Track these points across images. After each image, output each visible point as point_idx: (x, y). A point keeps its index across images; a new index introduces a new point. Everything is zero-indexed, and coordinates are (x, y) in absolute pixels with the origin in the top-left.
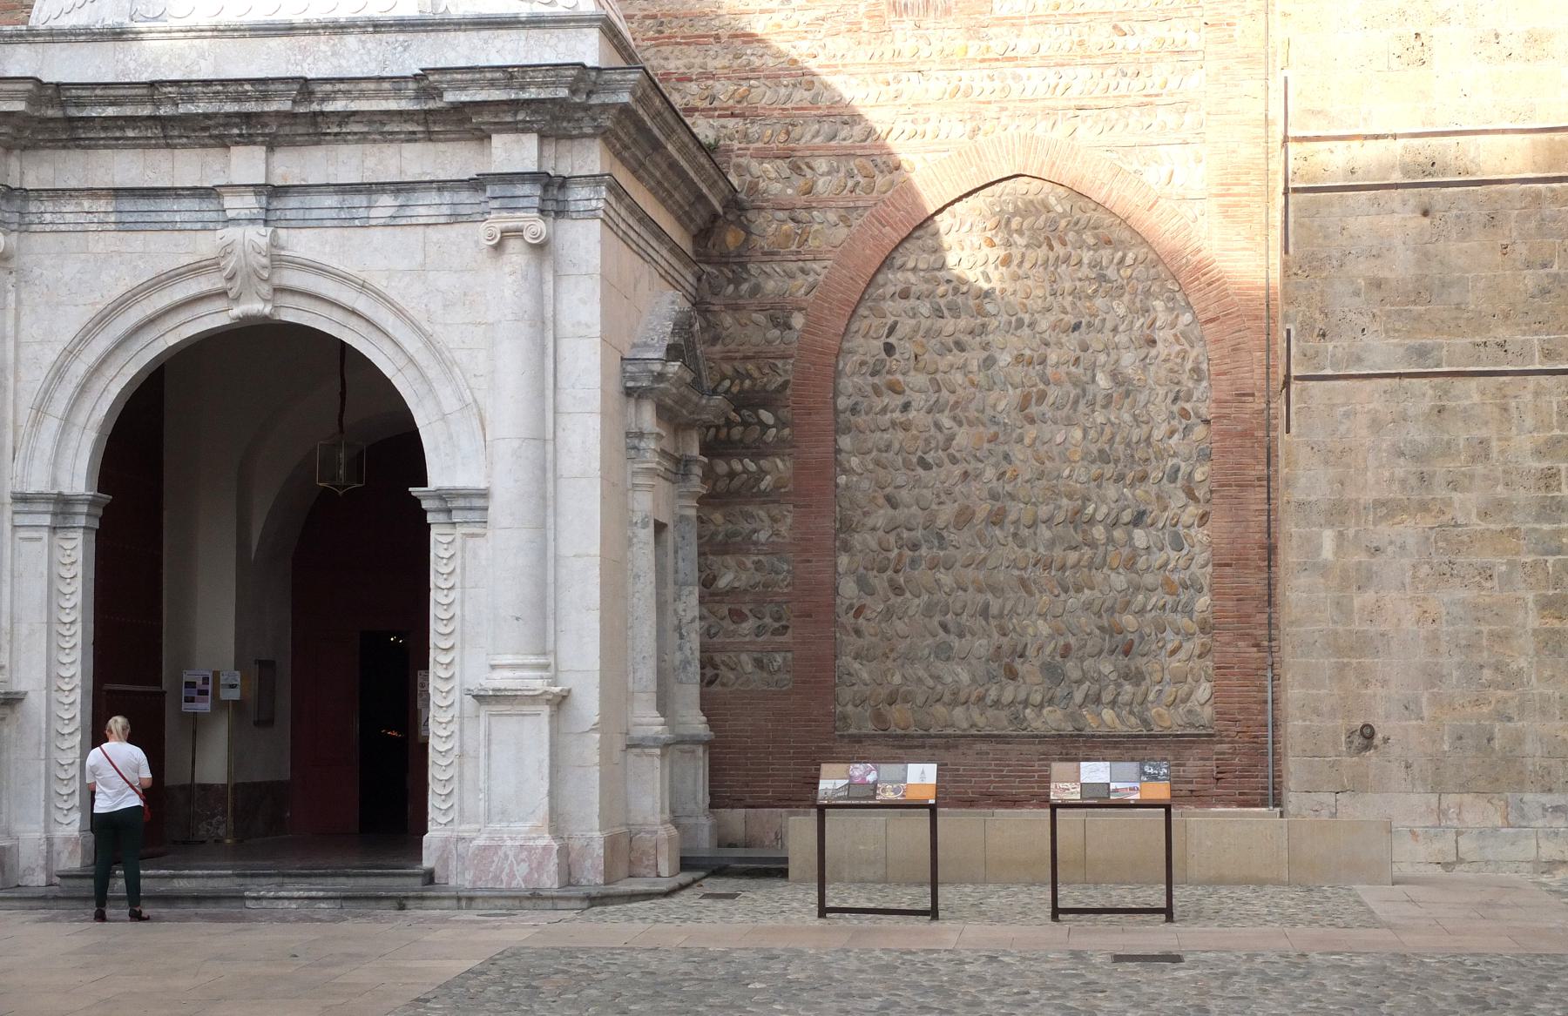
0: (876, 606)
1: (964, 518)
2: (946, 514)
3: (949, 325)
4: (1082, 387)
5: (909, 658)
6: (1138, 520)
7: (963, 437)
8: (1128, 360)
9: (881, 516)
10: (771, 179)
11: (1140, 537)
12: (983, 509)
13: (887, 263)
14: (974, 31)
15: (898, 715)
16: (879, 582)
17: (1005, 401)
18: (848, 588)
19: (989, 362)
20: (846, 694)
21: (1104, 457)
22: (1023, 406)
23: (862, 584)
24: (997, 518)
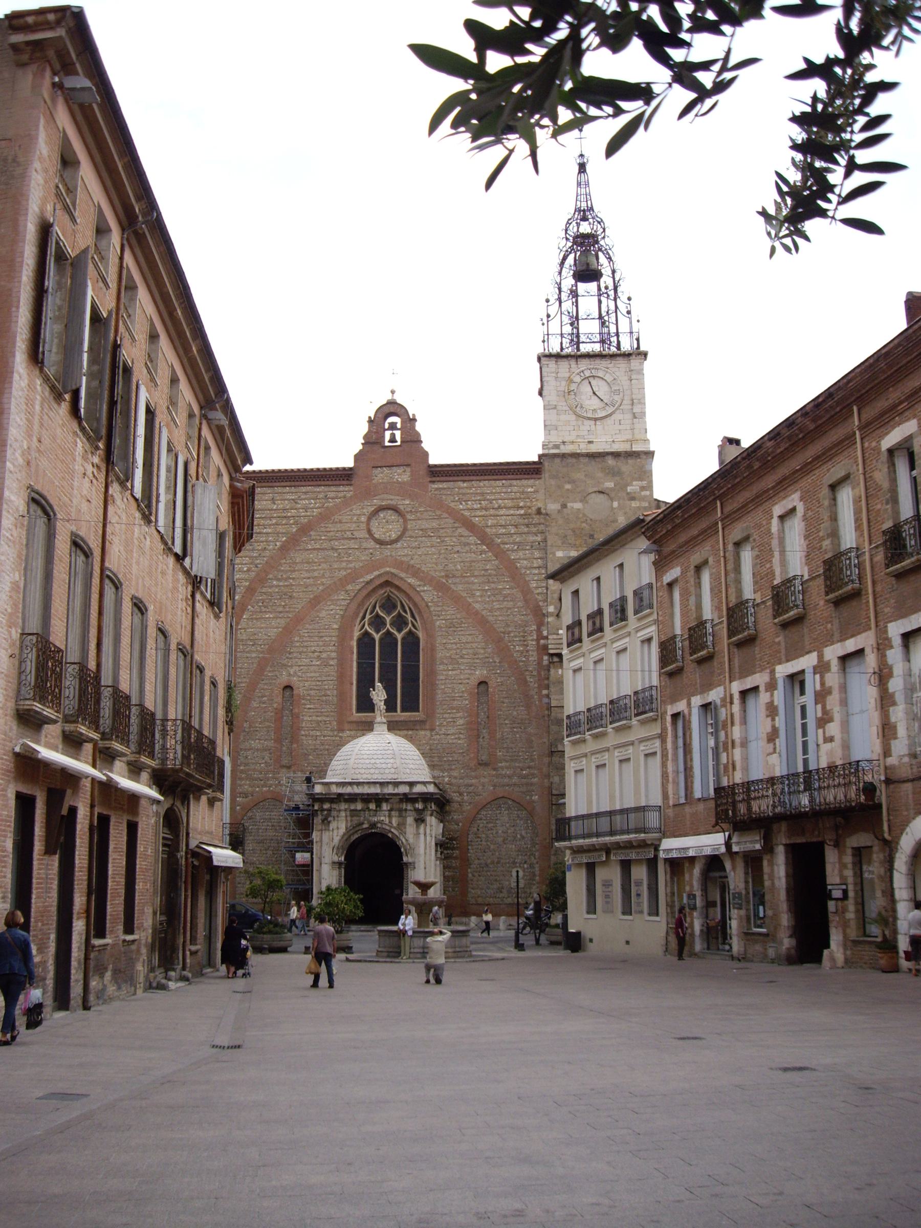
0: (475, 879)
1: (493, 863)
2: (489, 861)
3: (490, 825)
4: (515, 837)
5: (482, 889)
6: (525, 862)
7: (492, 847)
8: (523, 833)
9: (476, 862)
10: (455, 797)
11: (525, 866)
12: (496, 860)
13: (478, 813)
14: (495, 769)
15: (480, 900)
16: (476, 874)
17: (500, 840)
18: (470, 875)
19: (497, 833)
20: (470, 895)
21: (519, 851)
22: (504, 841)
23: (473, 876)
24: (498, 863)
